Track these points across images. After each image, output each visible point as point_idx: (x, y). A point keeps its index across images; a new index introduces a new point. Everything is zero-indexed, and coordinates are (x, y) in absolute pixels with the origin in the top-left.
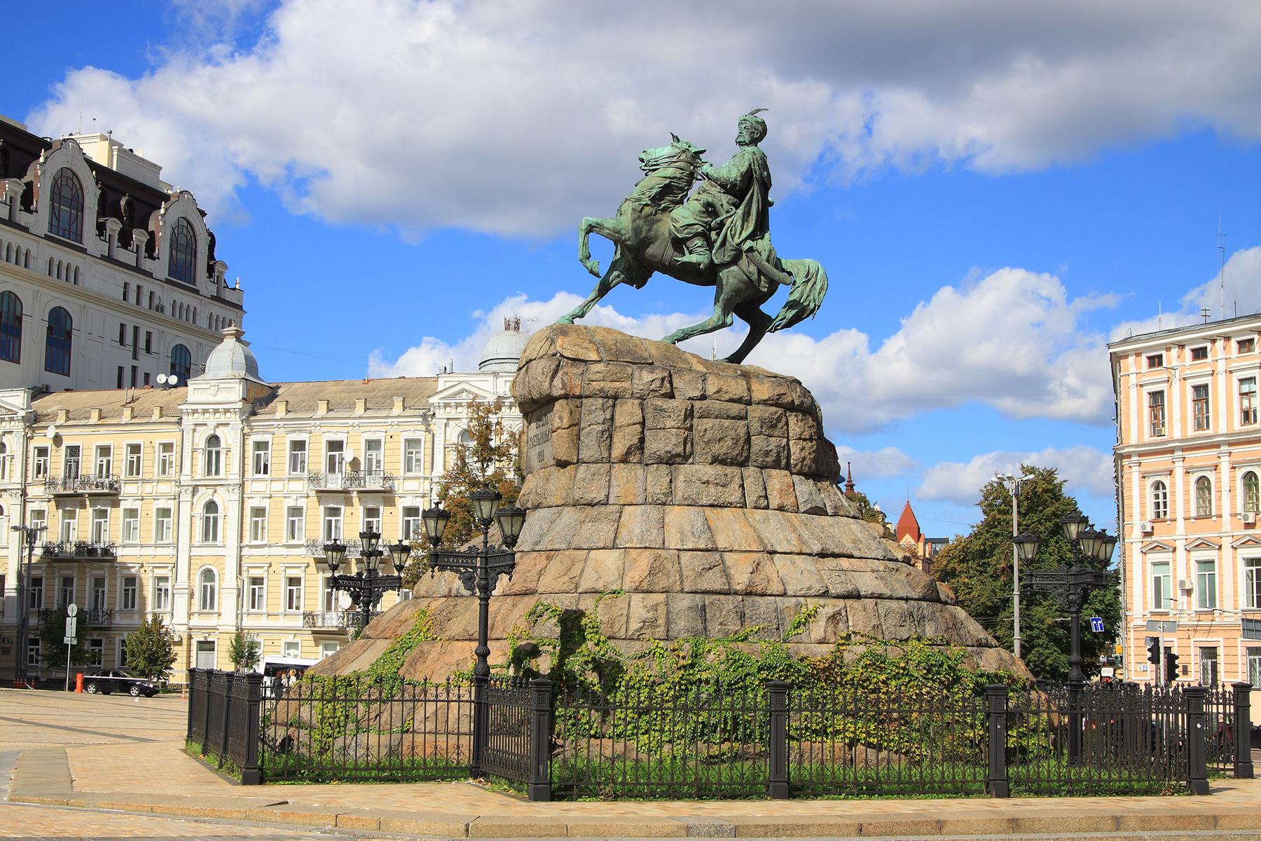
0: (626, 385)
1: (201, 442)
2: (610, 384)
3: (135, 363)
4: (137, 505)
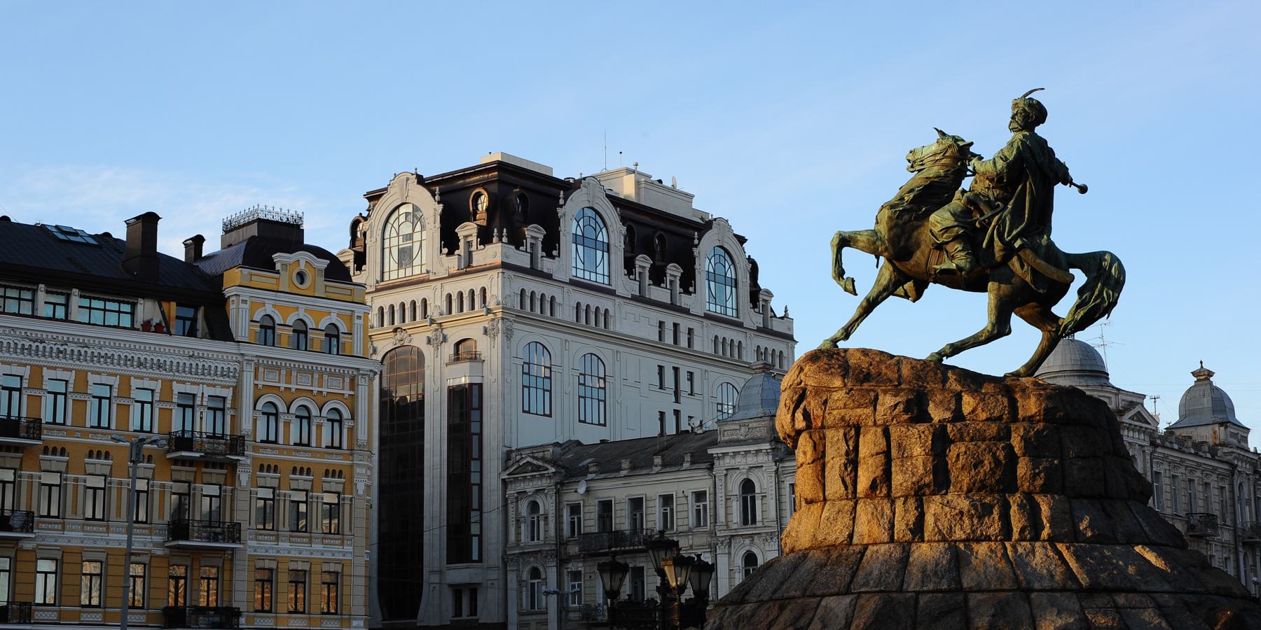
1: (735, 488)
3: (677, 407)
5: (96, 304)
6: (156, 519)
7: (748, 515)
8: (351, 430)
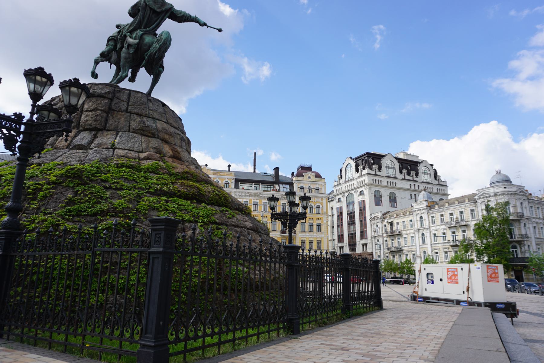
1: (419, 218)
4: (406, 236)
5: (271, 187)
6: (278, 230)
7: (422, 224)
8: (322, 209)
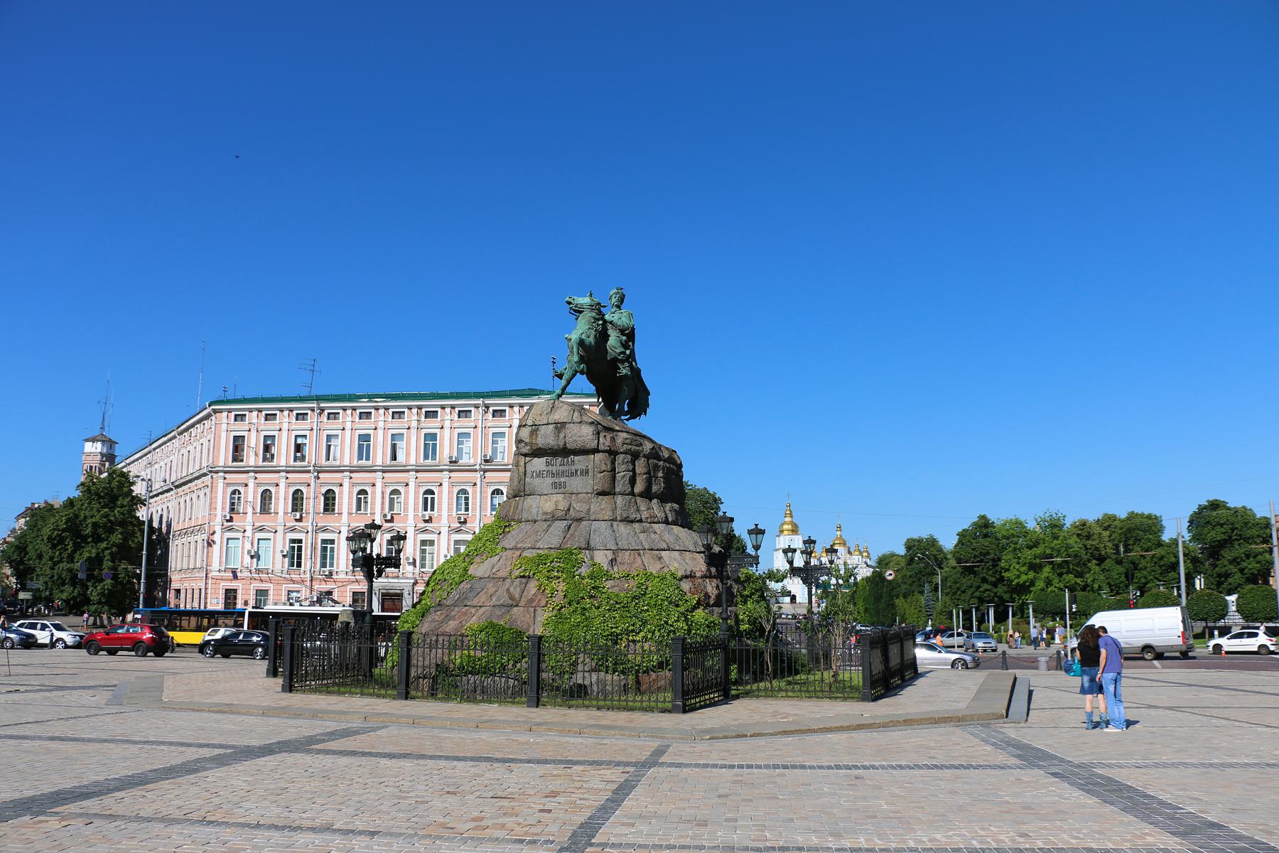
0: (641, 448)
2: (633, 447)
